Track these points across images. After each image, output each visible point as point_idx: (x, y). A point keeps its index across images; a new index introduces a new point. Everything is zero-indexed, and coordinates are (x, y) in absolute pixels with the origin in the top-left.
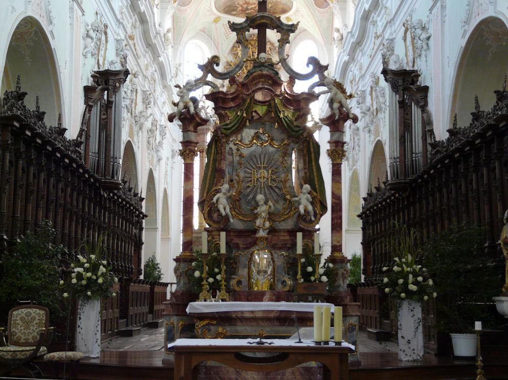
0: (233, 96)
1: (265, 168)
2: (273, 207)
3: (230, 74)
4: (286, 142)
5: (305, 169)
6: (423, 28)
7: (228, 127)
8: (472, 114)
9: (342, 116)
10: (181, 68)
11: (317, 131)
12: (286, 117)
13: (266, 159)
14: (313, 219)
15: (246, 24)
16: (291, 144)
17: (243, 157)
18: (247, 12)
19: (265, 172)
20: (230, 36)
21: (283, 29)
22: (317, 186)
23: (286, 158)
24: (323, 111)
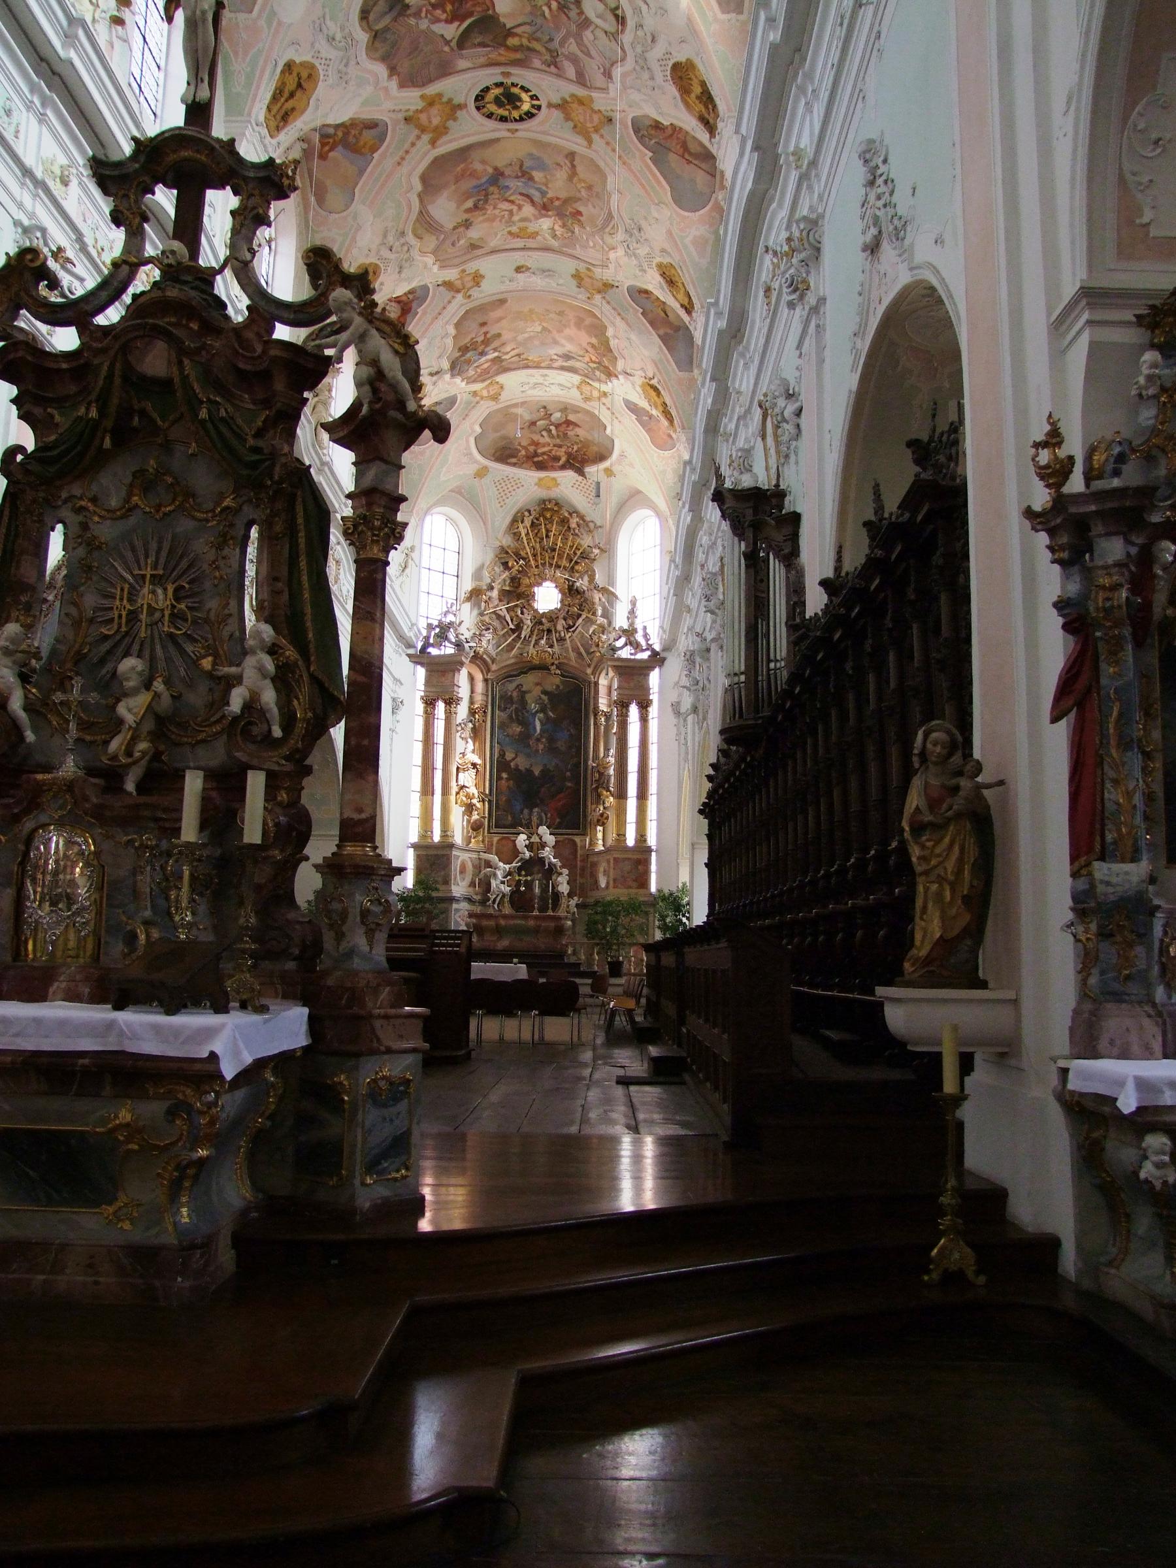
0: (74, 364)
1: (157, 580)
2: (166, 700)
3: (82, 305)
4: (227, 502)
5: (276, 579)
6: (790, 396)
7: (49, 454)
8: (865, 524)
9: (378, 406)
10: (414, 555)
11: (657, 670)
12: (222, 419)
13: (164, 554)
14: (277, 732)
16: (245, 508)
17: (99, 548)
18: (536, 459)
19: (160, 591)
21: (246, 179)
22: (311, 635)
23: (226, 551)
24: (664, 631)
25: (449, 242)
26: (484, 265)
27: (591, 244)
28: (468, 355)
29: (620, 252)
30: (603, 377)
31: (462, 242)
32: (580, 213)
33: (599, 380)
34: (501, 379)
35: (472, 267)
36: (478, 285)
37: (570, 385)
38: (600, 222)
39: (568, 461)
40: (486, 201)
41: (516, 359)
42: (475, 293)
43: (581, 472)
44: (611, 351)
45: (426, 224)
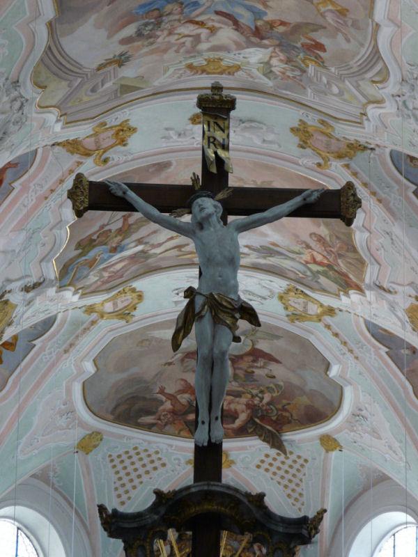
15: (156, 517)
20: (133, 494)
25: (89, 86)
26: (137, 115)
27: (335, 90)
28: (92, 254)
29: (390, 108)
30: (333, 287)
31: (108, 85)
32: (321, 47)
33: (324, 290)
34: (138, 285)
35: (114, 119)
36: (123, 142)
37: (265, 293)
38: (354, 64)
39: (250, 420)
40: (158, 24)
41: (175, 252)
42: (116, 155)
43: (275, 442)
44: (355, 250)
45: (55, 63)
